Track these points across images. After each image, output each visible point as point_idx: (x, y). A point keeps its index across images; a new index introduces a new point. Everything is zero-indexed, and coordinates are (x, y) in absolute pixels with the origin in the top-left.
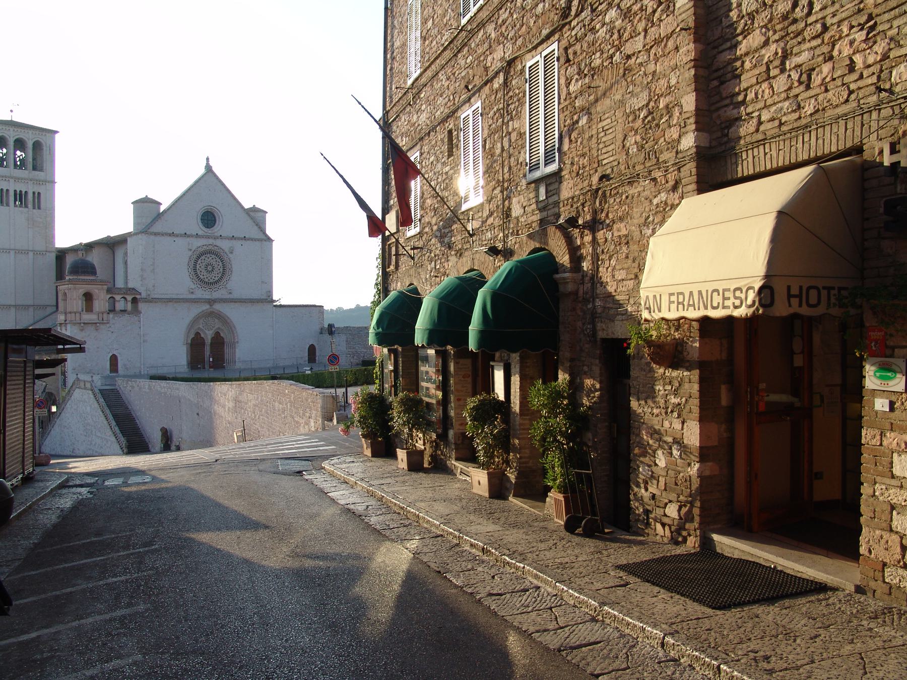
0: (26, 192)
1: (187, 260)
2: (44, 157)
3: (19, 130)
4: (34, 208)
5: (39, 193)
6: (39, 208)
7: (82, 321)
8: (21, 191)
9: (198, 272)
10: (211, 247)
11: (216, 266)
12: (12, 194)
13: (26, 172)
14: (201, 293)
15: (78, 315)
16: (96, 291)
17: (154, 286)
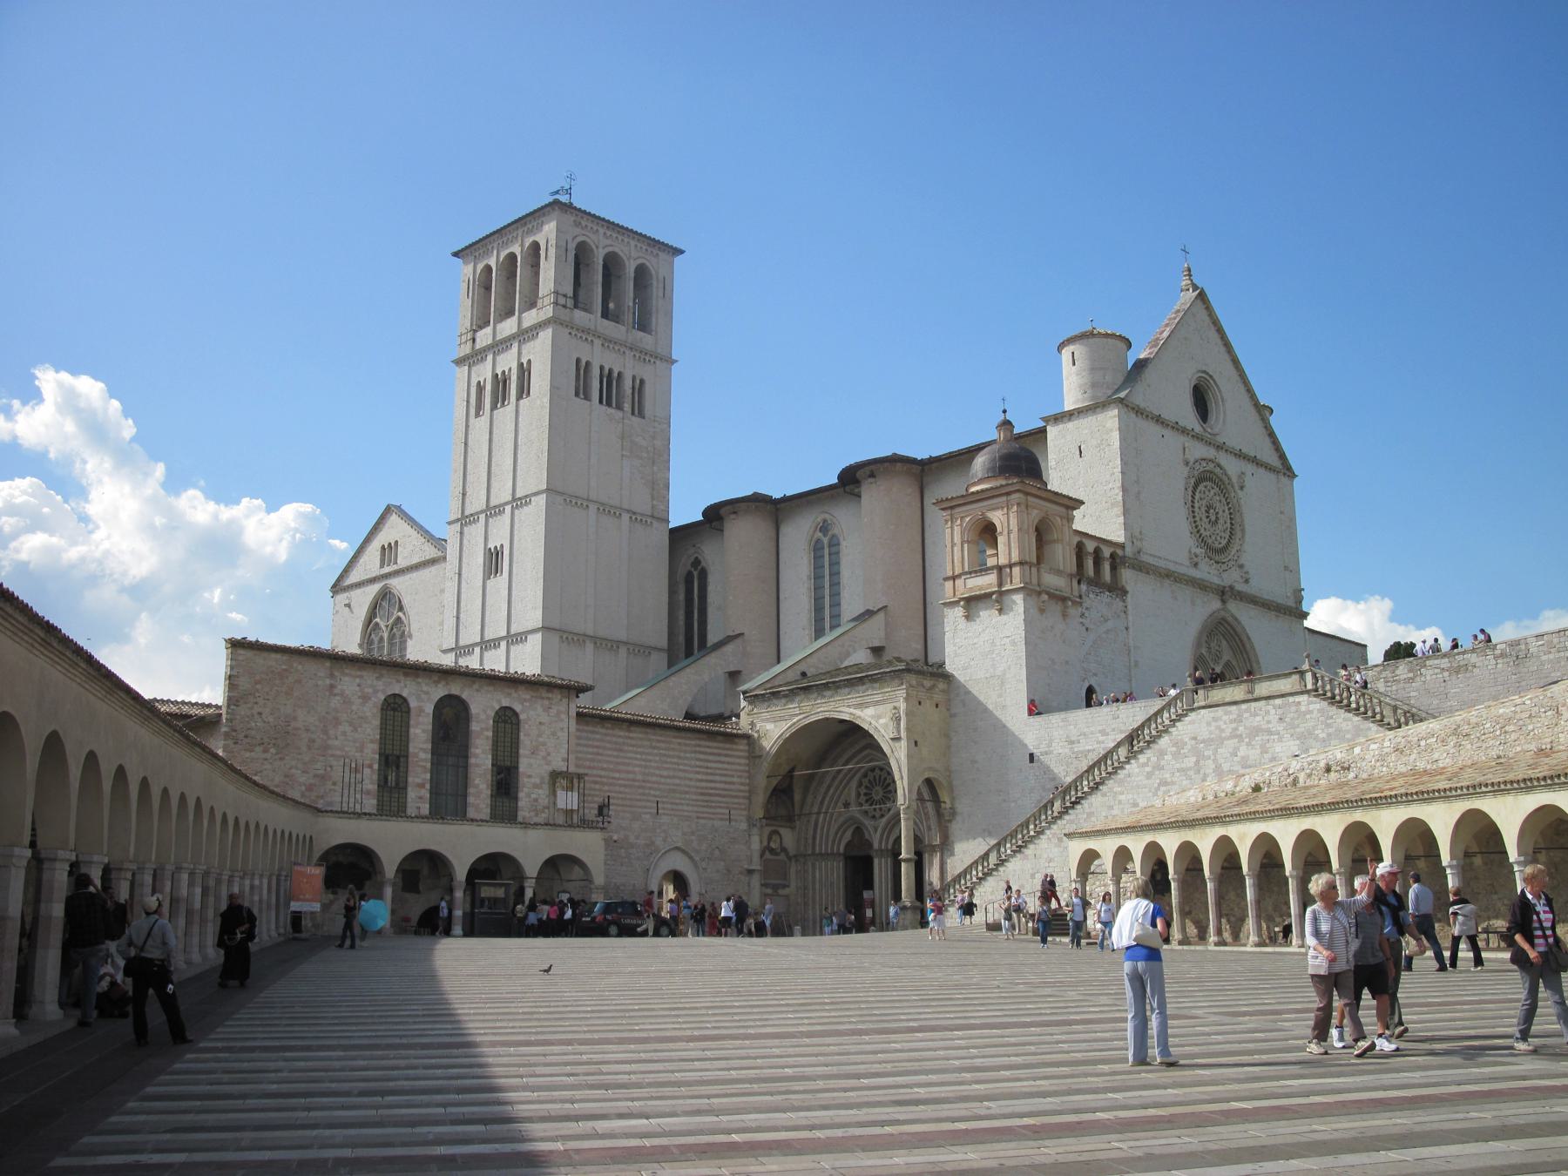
0: (620, 374)
1: (1182, 486)
2: (654, 302)
3: (615, 235)
4: (633, 413)
5: (642, 382)
6: (641, 415)
7: (1043, 587)
8: (610, 371)
9: (1197, 519)
10: (1211, 466)
11: (1221, 513)
12: (596, 372)
13: (623, 329)
15: (1034, 570)
16: (1059, 519)
17: (1141, 533)
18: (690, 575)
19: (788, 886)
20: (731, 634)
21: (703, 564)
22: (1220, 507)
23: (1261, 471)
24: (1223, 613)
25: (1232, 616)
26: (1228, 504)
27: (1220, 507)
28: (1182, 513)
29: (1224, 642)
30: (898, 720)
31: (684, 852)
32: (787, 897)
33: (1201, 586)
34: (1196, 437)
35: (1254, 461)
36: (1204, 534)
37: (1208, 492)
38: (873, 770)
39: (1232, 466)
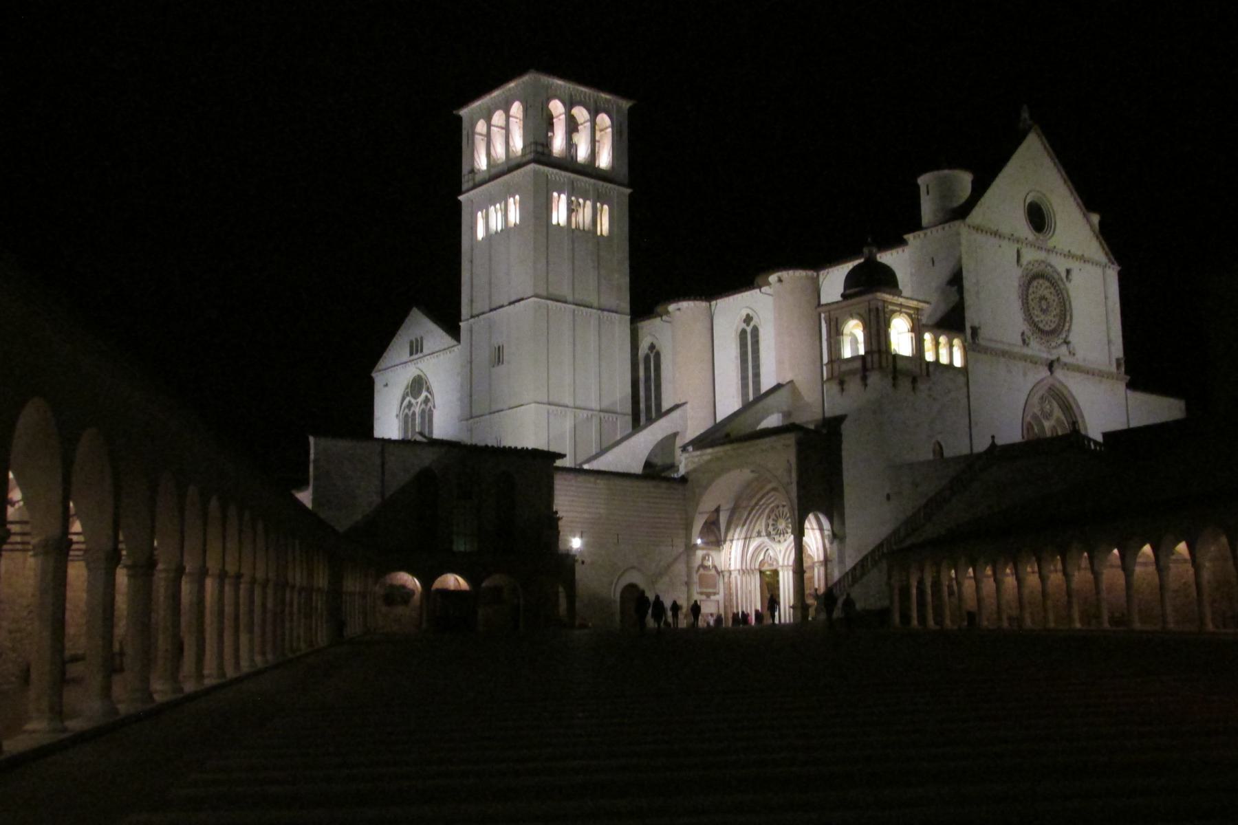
14: (1036, 348)
18: (647, 358)
19: (718, 594)
20: (678, 402)
21: (657, 347)
22: (1051, 298)
23: (1088, 267)
24: (1050, 380)
25: (1060, 382)
26: (1058, 295)
27: (1053, 299)
28: (1016, 305)
29: (1055, 404)
30: (790, 471)
31: (639, 570)
32: (718, 602)
33: (1034, 361)
34: (1032, 245)
35: (1083, 259)
36: (1036, 319)
37: (1042, 288)
38: (778, 507)
39: (1061, 265)
